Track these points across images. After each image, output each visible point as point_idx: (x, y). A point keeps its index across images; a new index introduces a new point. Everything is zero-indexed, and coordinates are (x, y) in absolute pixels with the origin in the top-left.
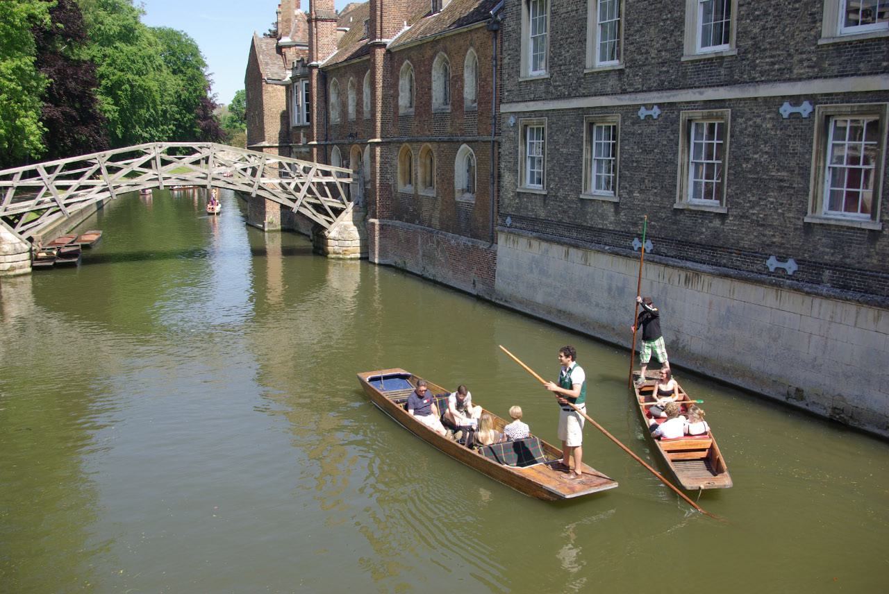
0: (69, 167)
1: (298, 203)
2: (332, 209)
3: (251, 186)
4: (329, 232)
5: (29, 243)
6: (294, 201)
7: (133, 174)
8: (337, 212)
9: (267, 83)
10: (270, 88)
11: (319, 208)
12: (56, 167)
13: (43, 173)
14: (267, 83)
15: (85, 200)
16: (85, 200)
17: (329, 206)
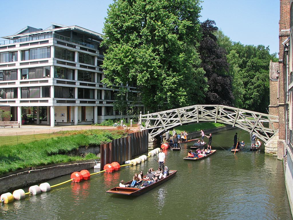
0: (174, 113)
1: (252, 130)
2: (268, 134)
3: (233, 122)
4: (266, 144)
5: (154, 139)
6: (251, 129)
7: (192, 117)
8: (270, 135)
9: (272, 81)
10: (273, 83)
11: (262, 133)
12: (170, 113)
13: (159, 116)
14: (272, 81)
15: (172, 125)
16: (172, 125)
17: (267, 133)
